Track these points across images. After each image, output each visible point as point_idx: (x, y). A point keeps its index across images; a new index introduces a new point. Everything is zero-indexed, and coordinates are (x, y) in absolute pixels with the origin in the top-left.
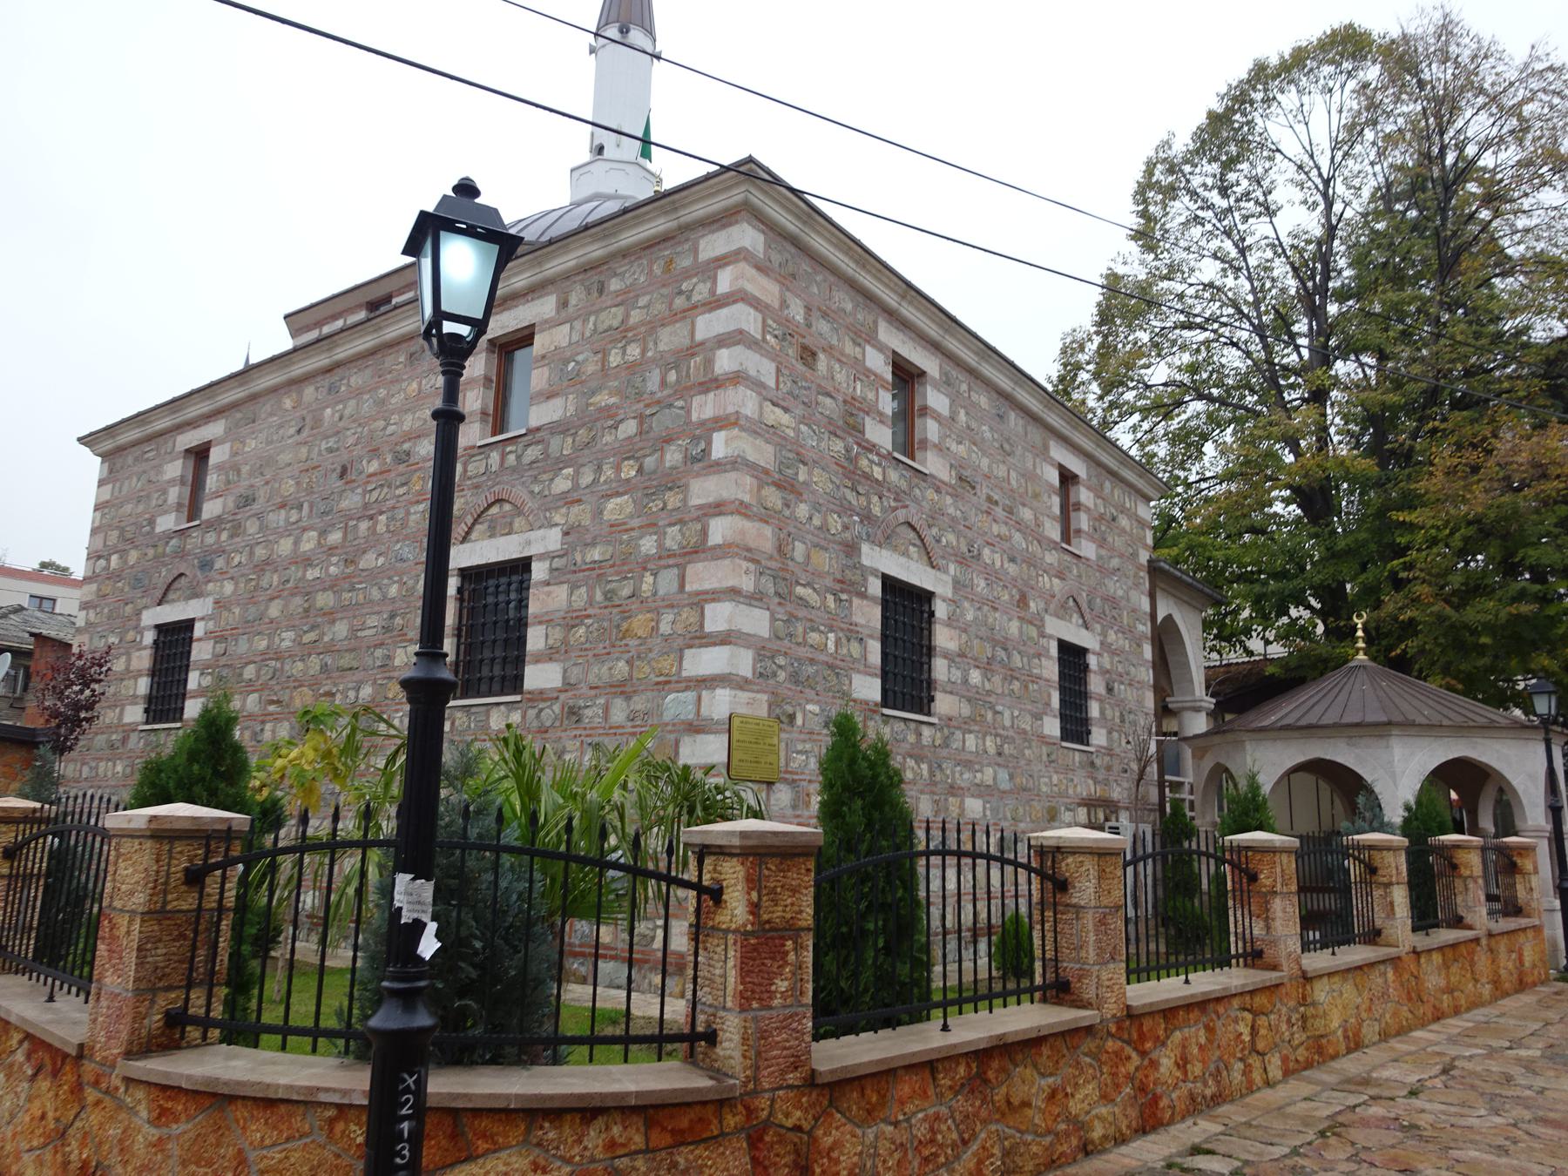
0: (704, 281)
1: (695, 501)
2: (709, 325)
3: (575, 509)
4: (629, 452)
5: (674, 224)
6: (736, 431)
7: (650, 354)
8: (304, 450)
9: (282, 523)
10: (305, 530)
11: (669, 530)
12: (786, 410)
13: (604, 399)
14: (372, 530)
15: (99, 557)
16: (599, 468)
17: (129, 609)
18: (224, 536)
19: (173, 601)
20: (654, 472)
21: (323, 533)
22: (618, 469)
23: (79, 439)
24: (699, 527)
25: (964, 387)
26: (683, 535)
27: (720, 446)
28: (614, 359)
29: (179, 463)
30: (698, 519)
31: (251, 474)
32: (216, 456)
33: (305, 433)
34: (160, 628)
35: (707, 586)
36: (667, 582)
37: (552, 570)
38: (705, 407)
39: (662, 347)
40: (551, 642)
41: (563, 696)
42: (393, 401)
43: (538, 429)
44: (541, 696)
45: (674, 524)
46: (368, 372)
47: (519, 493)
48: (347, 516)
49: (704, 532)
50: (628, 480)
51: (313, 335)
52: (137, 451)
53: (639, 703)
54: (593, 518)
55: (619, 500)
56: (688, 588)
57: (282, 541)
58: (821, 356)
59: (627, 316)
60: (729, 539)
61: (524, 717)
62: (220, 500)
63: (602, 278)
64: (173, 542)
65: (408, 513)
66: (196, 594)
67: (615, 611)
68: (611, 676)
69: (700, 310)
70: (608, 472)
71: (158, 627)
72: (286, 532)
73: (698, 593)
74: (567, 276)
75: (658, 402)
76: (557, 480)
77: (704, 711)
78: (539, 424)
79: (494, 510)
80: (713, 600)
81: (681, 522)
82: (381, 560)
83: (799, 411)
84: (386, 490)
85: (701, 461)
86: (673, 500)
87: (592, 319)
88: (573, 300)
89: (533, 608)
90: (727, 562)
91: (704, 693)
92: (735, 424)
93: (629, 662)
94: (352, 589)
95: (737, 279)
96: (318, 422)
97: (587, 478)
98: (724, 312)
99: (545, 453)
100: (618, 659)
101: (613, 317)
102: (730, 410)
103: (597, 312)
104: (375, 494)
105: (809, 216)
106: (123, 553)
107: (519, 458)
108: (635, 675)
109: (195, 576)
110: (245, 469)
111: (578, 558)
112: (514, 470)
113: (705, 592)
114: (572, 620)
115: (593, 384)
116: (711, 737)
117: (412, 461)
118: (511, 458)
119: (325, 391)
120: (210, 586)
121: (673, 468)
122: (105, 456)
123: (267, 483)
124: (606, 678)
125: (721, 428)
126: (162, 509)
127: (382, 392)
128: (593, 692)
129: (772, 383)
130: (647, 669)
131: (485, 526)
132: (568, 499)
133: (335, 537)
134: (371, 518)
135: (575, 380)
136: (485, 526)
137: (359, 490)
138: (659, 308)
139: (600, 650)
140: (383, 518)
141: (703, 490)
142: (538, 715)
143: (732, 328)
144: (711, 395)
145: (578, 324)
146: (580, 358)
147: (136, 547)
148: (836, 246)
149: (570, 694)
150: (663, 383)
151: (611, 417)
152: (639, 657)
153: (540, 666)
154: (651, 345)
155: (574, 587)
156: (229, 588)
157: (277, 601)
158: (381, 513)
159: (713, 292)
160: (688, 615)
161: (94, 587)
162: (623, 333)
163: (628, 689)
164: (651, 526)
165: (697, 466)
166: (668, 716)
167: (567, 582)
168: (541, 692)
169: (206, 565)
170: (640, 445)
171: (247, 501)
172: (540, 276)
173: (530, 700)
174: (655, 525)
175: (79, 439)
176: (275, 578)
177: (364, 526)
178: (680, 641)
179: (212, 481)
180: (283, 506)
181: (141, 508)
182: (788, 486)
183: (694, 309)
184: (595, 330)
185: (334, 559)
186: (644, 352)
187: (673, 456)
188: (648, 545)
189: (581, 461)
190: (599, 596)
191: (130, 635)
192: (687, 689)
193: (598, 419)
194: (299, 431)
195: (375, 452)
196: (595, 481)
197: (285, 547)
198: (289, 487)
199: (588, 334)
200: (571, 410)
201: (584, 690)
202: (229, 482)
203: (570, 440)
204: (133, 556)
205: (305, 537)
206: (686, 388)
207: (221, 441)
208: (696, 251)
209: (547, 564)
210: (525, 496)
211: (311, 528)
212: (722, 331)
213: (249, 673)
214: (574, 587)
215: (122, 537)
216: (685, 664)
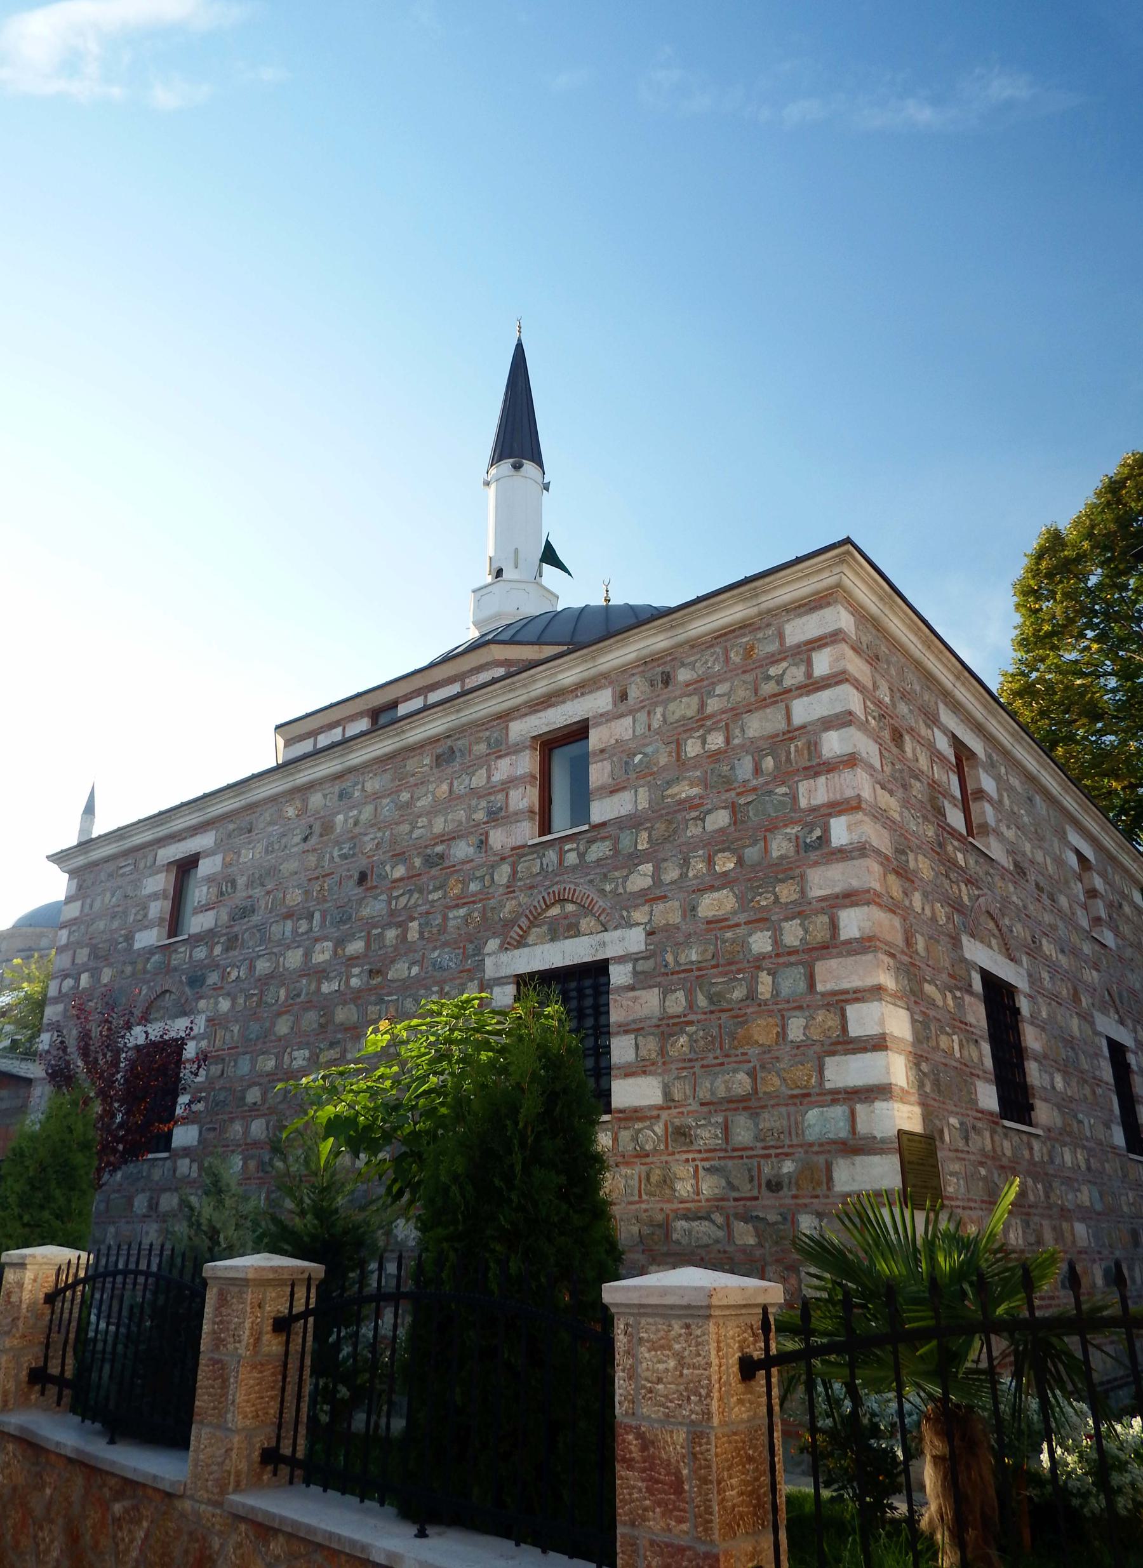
0: (795, 665)
1: (816, 892)
2: (805, 710)
3: (659, 907)
4: (720, 842)
5: (755, 610)
6: (860, 816)
7: (736, 741)
8: (312, 859)
9: (288, 934)
10: (317, 940)
11: (786, 925)
12: (891, 793)
13: (685, 791)
14: (403, 938)
15: (66, 976)
16: (686, 863)
18: (218, 950)
20: (759, 864)
21: (340, 943)
22: (710, 861)
23: (48, 857)
24: (826, 919)
25: (1003, 770)
26: (806, 931)
27: (840, 832)
28: (692, 748)
29: (164, 874)
30: (822, 911)
31: (250, 884)
32: (206, 867)
33: (313, 841)
35: (845, 985)
36: (792, 982)
37: (635, 973)
38: (815, 792)
39: (751, 733)
40: (643, 1053)
41: (665, 1115)
42: (419, 804)
43: (603, 824)
44: (634, 1115)
45: (793, 918)
46: (388, 776)
47: (584, 890)
48: (370, 924)
49: (834, 926)
50: (725, 874)
51: (306, 746)
52: (110, 867)
53: (770, 1120)
54: (684, 916)
55: (716, 895)
56: (820, 988)
57: (289, 953)
58: (907, 738)
59: (702, 706)
60: (868, 932)
61: (615, 1140)
62: (211, 914)
63: (668, 669)
64: (156, 958)
65: (445, 918)
66: (184, 1011)
67: (724, 1016)
68: (728, 1089)
69: (794, 693)
70: (698, 866)
72: (295, 942)
73: (834, 993)
74: (625, 670)
75: (755, 789)
76: (632, 877)
77: (862, 1128)
78: (603, 819)
79: (555, 911)
80: (857, 1000)
81: (800, 914)
82: (415, 970)
83: (900, 793)
84: (416, 895)
85: (819, 848)
86: (787, 892)
87: (659, 710)
88: (634, 693)
89: (616, 1016)
90: (870, 957)
91: (859, 1107)
92: (858, 808)
93: (752, 1074)
94: (381, 1001)
95: (837, 660)
97: (671, 874)
98: (825, 694)
99: (616, 850)
100: (735, 1071)
101: (686, 707)
102: (849, 793)
103: (665, 703)
104: (403, 901)
105: (890, 597)
106: (95, 974)
107: (581, 856)
108: (761, 1089)
109: (183, 993)
110: (241, 881)
111: (670, 958)
112: (574, 868)
113: (846, 992)
114: (667, 1028)
115: (667, 776)
116: (876, 1159)
117: (447, 863)
118: (572, 858)
119: (336, 798)
120: (202, 1004)
121: (781, 857)
122: (73, 873)
123: (268, 893)
124: (721, 1093)
125: (840, 813)
126: (143, 924)
127: (405, 796)
128: (705, 1109)
129: (878, 765)
130: (776, 1081)
131: (545, 928)
132: (648, 897)
133: (356, 947)
134: (399, 925)
135: (646, 773)
136: (545, 928)
137: (384, 897)
138: (742, 694)
139: (710, 1060)
140: (414, 925)
141: (824, 880)
142: (635, 1139)
143: (838, 709)
144: (822, 779)
145: (642, 716)
146: (649, 750)
147: (110, 965)
148: (909, 627)
149: (674, 1111)
150: (757, 770)
151: (694, 807)
152: (763, 1067)
153: (631, 1081)
154: (737, 732)
155: (666, 992)
156: (225, 1005)
157: (285, 1017)
158: (412, 919)
159: (809, 674)
160: (826, 1019)
161: (60, 1007)
162: (701, 723)
163: (753, 1103)
164: (761, 921)
165: (813, 856)
166: (811, 1135)
167: (658, 985)
168: (636, 1110)
169: (196, 981)
170: (737, 834)
171: (244, 912)
172: (593, 672)
173: (620, 1119)
174: (766, 919)
175: (48, 857)
176: (283, 993)
177: (391, 934)
178: (817, 1048)
179: (198, 893)
180: (289, 916)
181: (116, 924)
182: (904, 874)
183: (784, 695)
184: (665, 721)
185: (356, 971)
186: (728, 741)
187: (780, 846)
188: (761, 942)
189: (661, 856)
190: (702, 1001)
192: (834, 1102)
193: (679, 810)
194: (305, 839)
195: (400, 857)
196: (683, 876)
197: (294, 959)
198: (295, 897)
199: (655, 725)
200: (643, 804)
201: (694, 1106)
202: (222, 894)
203: (644, 835)
204: (106, 975)
205: (318, 947)
206: (787, 773)
208: (781, 636)
209: (629, 967)
210: (594, 895)
211: (326, 938)
212: (825, 714)
213: (253, 1095)
214: (666, 992)
215: (94, 954)
216: (828, 1074)
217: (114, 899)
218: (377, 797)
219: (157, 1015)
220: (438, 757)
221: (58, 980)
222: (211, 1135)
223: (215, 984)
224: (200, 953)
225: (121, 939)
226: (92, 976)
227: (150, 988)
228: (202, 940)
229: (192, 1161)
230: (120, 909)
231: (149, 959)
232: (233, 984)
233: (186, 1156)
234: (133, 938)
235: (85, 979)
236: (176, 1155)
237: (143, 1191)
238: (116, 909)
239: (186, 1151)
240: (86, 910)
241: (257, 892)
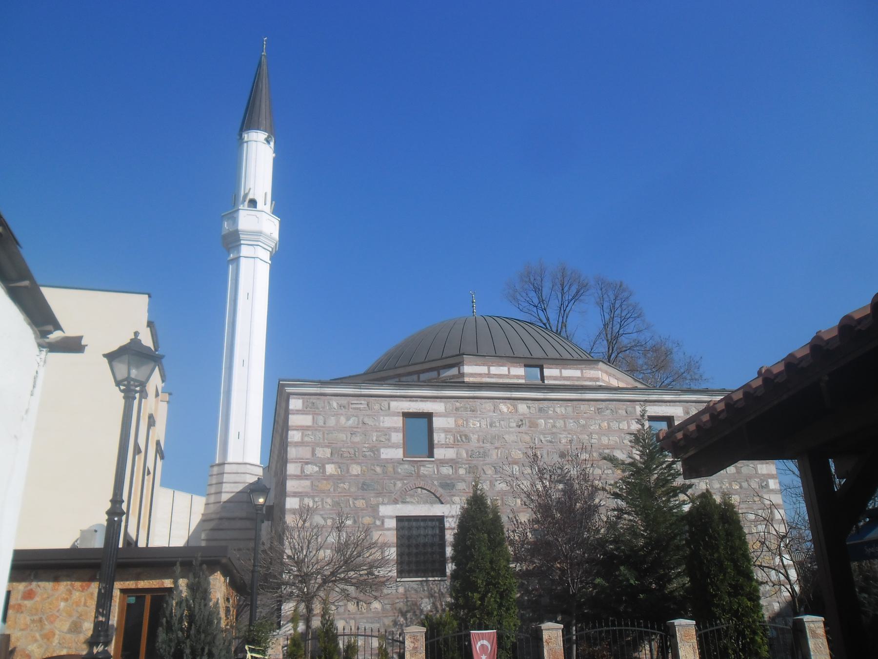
15: (307, 463)
33: (523, 428)
34: (400, 519)
71: (397, 517)
96: (533, 425)
110: (474, 437)
161: (307, 483)
181: (357, 439)
202: (458, 441)
207: (440, 415)
217: (351, 422)
218: (564, 417)
219: (412, 500)
220: (598, 409)
221: (300, 465)
224: (446, 470)
227: (404, 484)
228: (447, 463)
230: (359, 430)
234: (378, 451)
235: (330, 469)
240: (321, 423)
241: (488, 446)
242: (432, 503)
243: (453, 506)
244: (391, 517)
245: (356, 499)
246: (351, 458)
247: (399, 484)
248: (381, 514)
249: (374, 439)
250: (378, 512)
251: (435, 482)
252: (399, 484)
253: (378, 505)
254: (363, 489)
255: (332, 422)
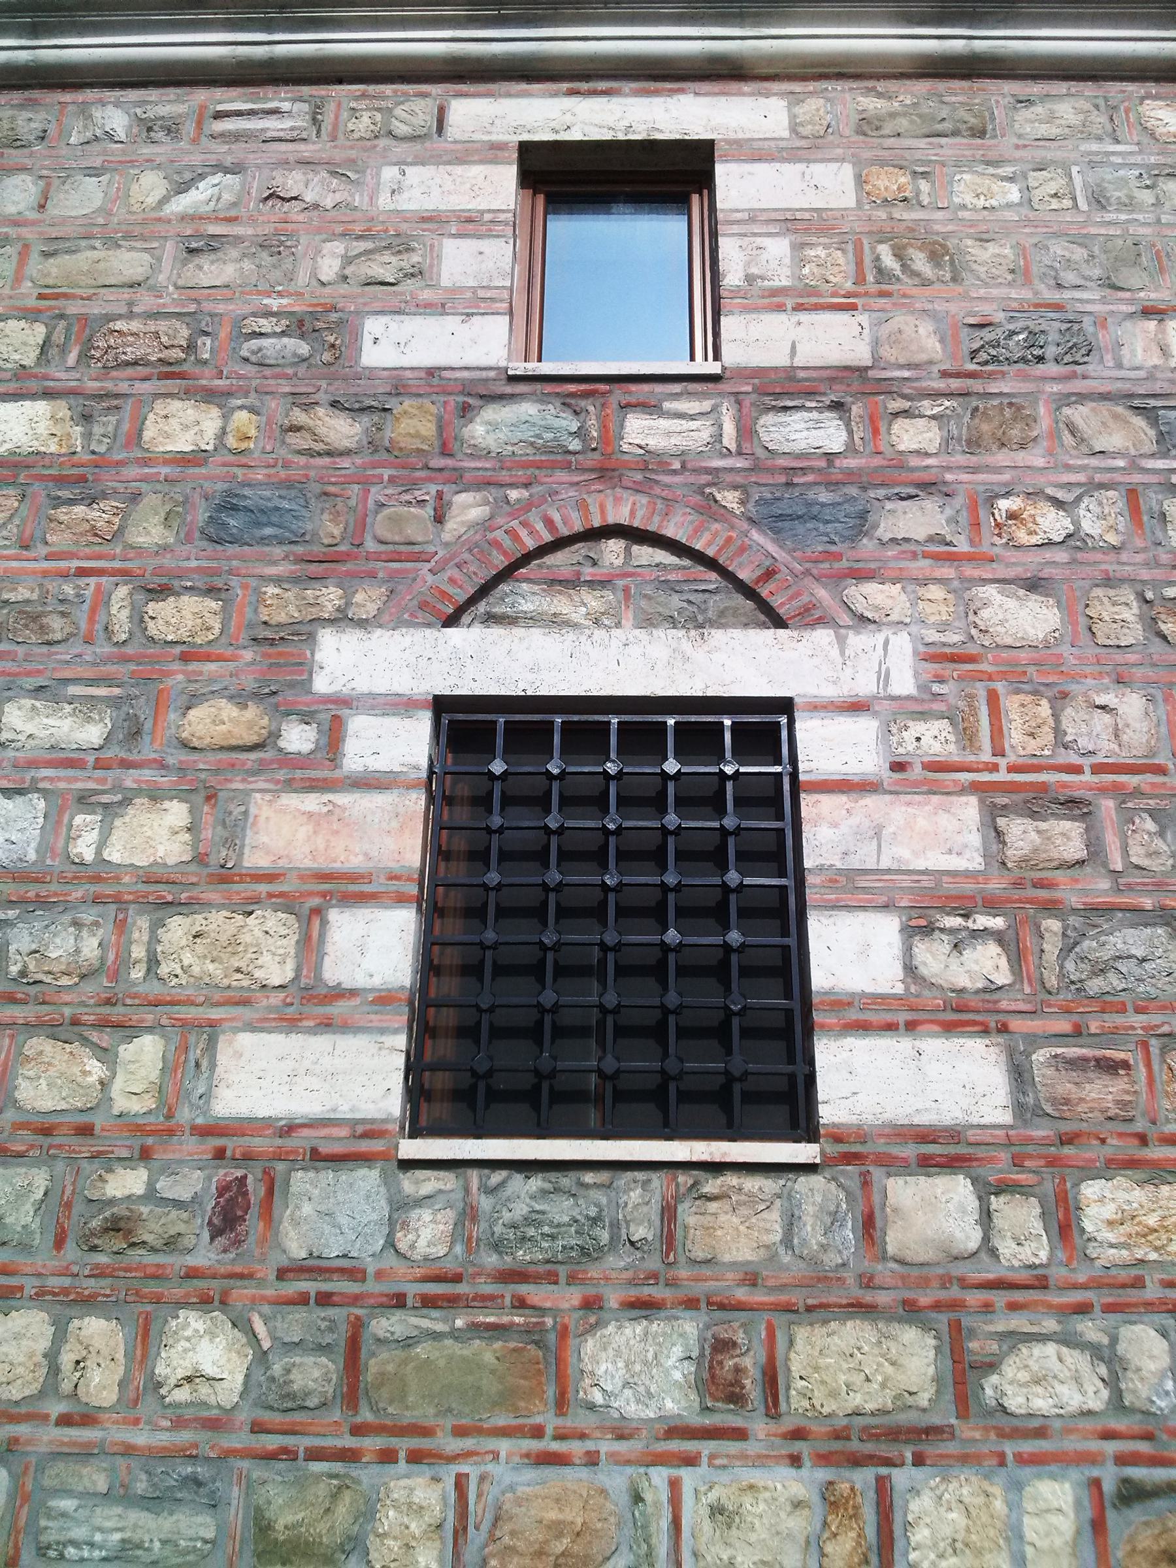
17: (182, 617)
19: (556, 622)
34: (464, 724)
71: (442, 705)
120: (872, 595)
147: (209, 396)
181: (213, 272)
191: (215, 720)
207: (755, 152)
217: (198, 197)
219: (560, 604)
222: (1101, 1092)
223: (934, 539)
225: (266, 325)
226: (86, 418)
228: (810, 394)
229: (987, 1191)
231: (465, 411)
232: (1062, 556)
233: (927, 1165)
236: (861, 1156)
237: (643, 1307)
238: (213, 229)
239: (939, 1150)
241: (1091, 300)
242: (698, 622)
243: (858, 641)
244: (402, 705)
245: (161, 592)
246: (169, 371)
247: (468, 509)
248: (322, 684)
249: (329, 268)
250: (305, 668)
251: (729, 499)
252: (468, 509)
253: (303, 633)
254: (217, 535)
255: (83, 198)
